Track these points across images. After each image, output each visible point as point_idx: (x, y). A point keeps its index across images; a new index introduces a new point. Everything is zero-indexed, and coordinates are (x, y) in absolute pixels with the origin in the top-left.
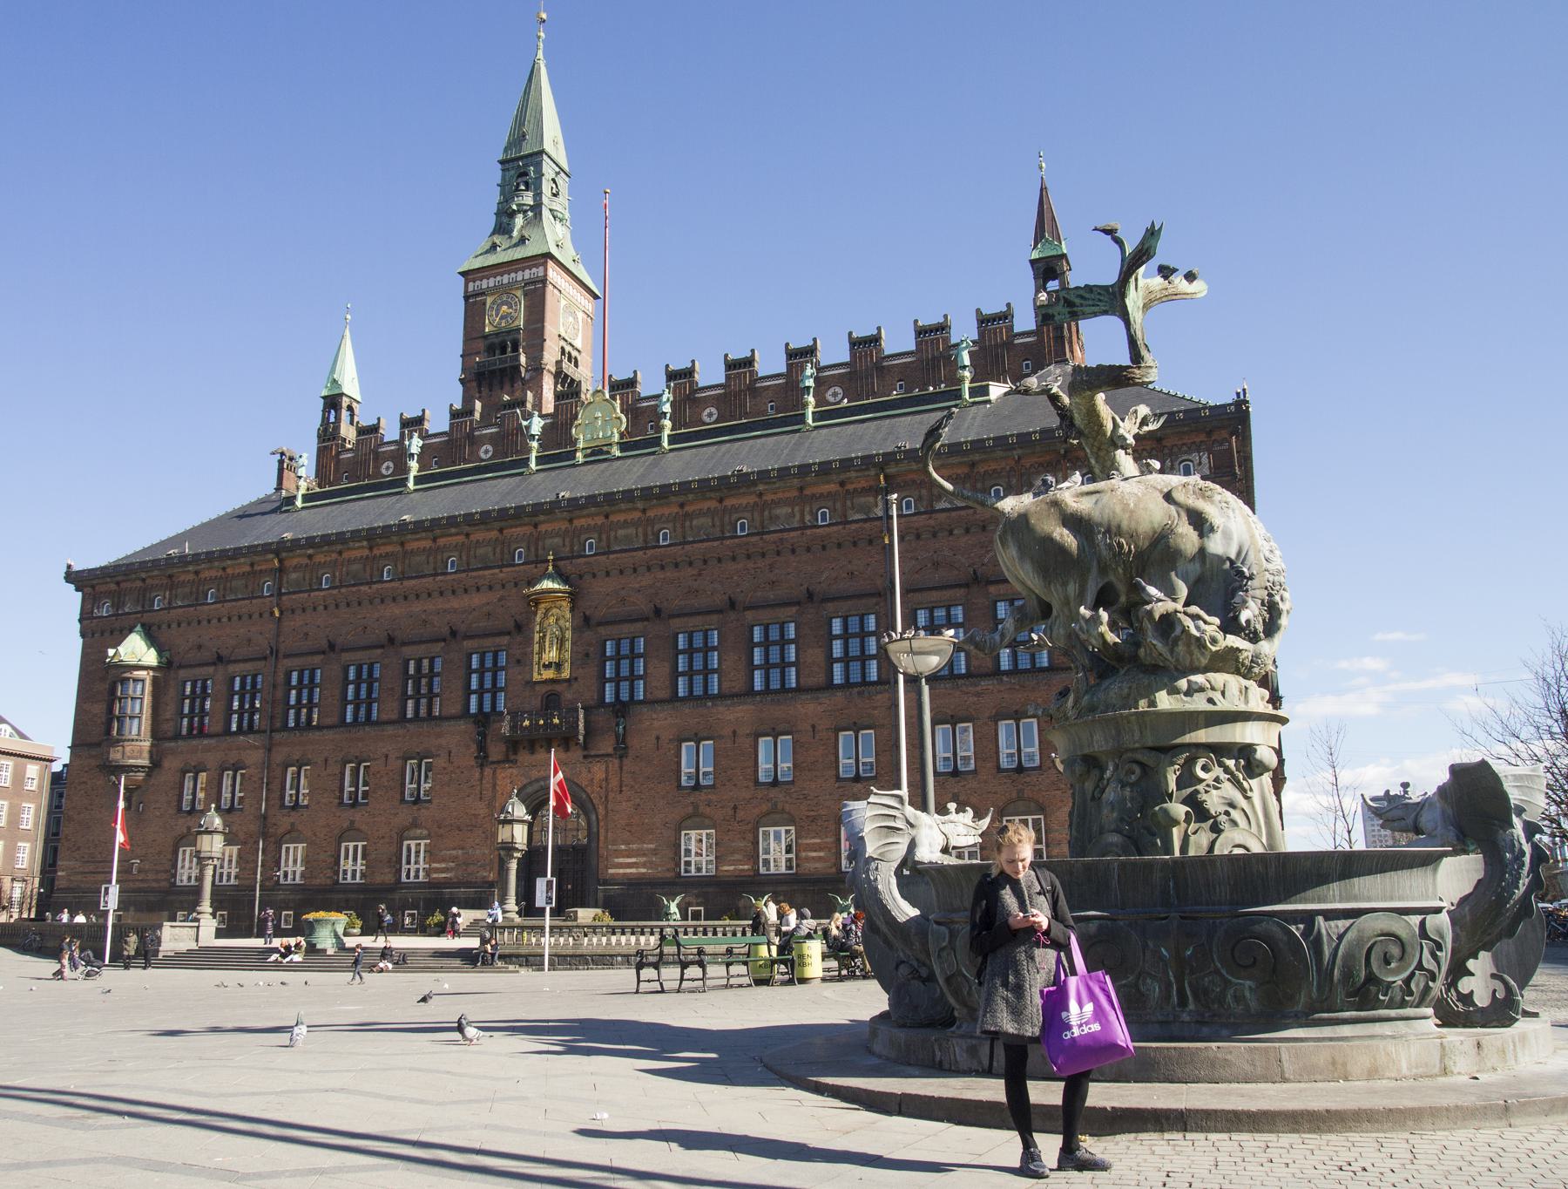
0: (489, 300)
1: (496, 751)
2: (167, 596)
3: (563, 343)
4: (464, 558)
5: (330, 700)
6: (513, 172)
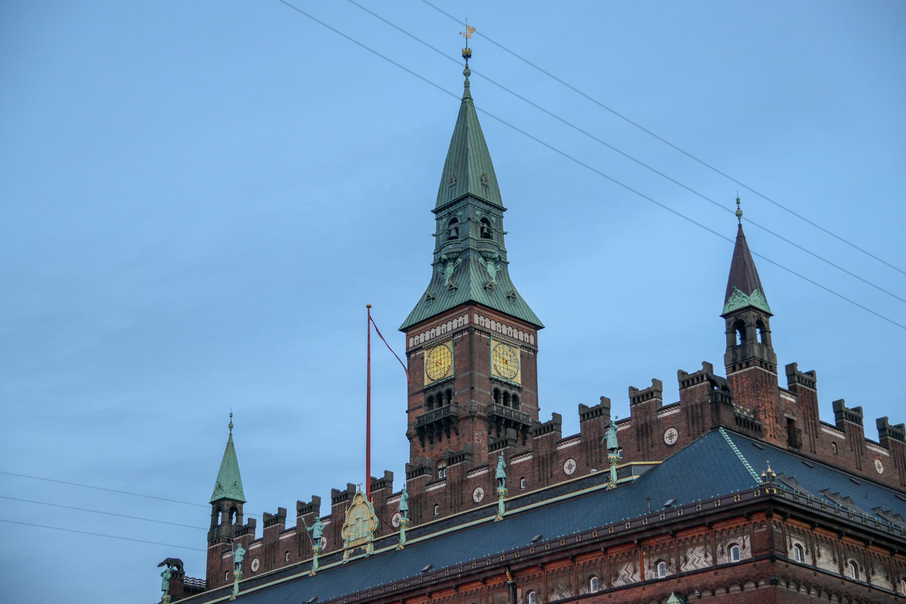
0: (426, 353)
3: (495, 385)
6: (445, 220)
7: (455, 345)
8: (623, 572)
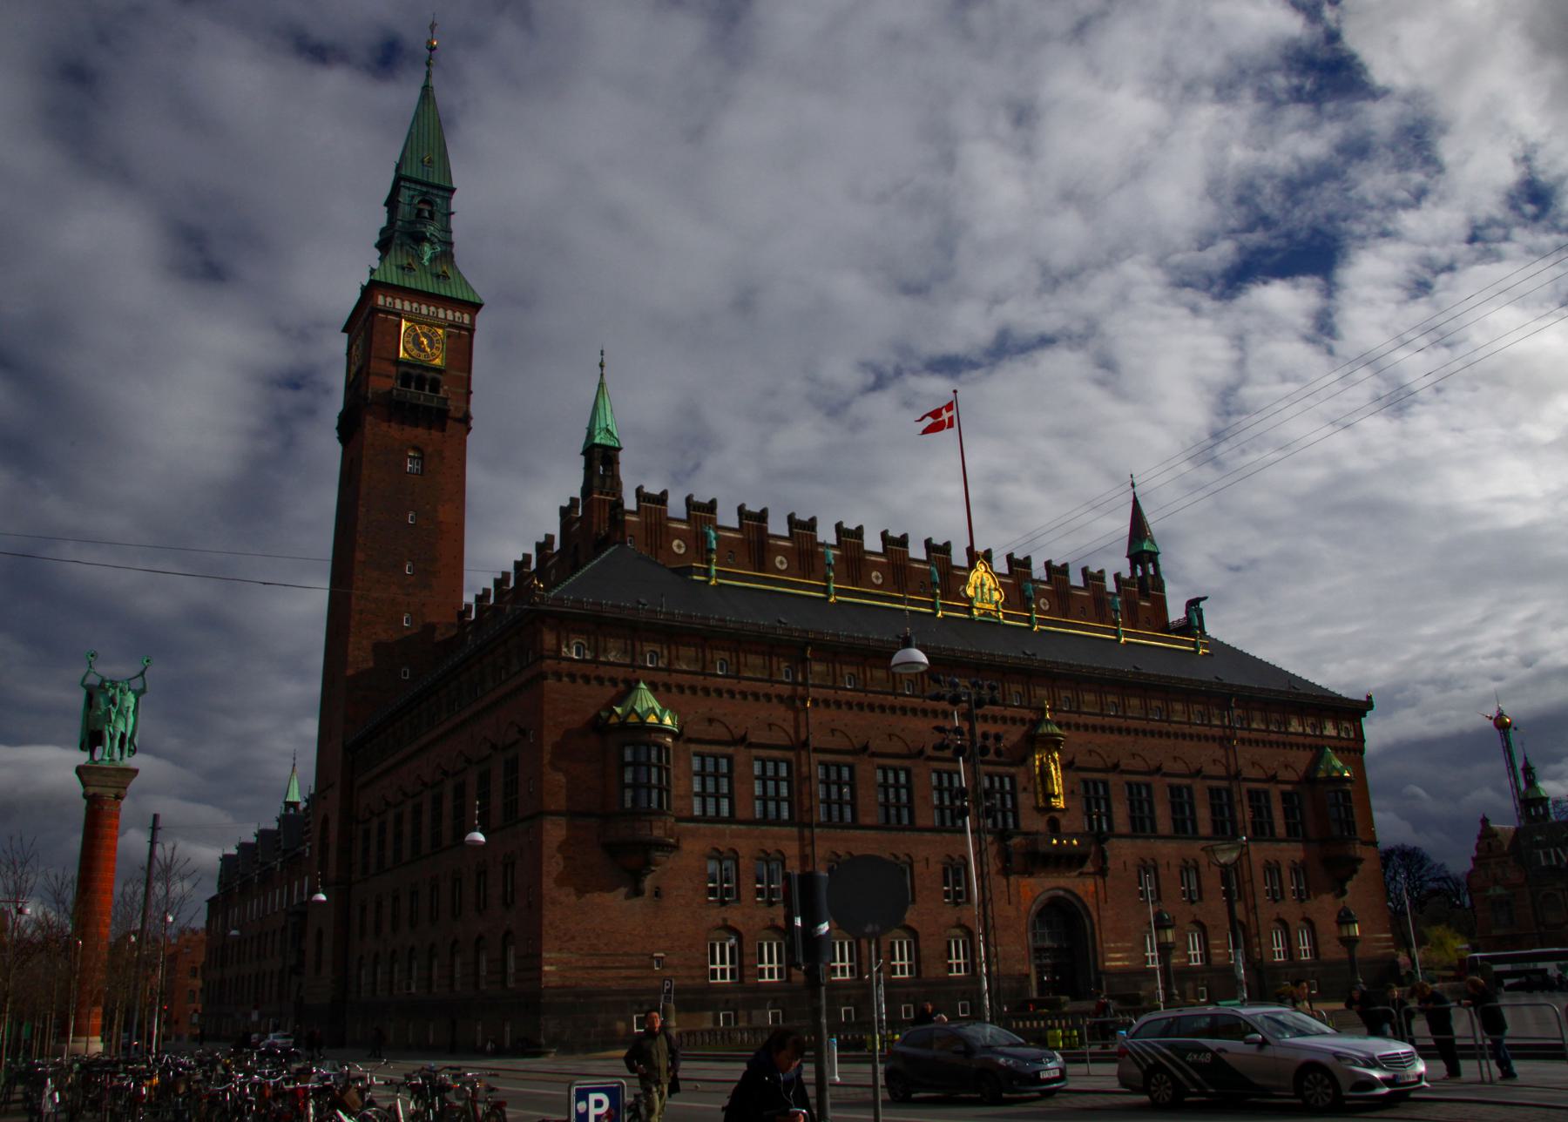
7: (449, 336)
8: (1293, 724)
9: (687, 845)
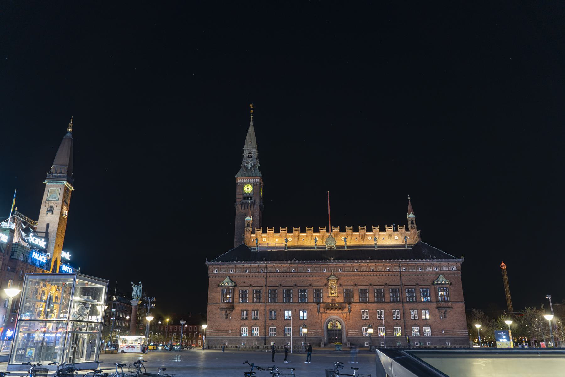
1: (322, 310)
2: (235, 270)
4: (312, 269)
5: (280, 297)
8: (428, 268)
9: (237, 308)
